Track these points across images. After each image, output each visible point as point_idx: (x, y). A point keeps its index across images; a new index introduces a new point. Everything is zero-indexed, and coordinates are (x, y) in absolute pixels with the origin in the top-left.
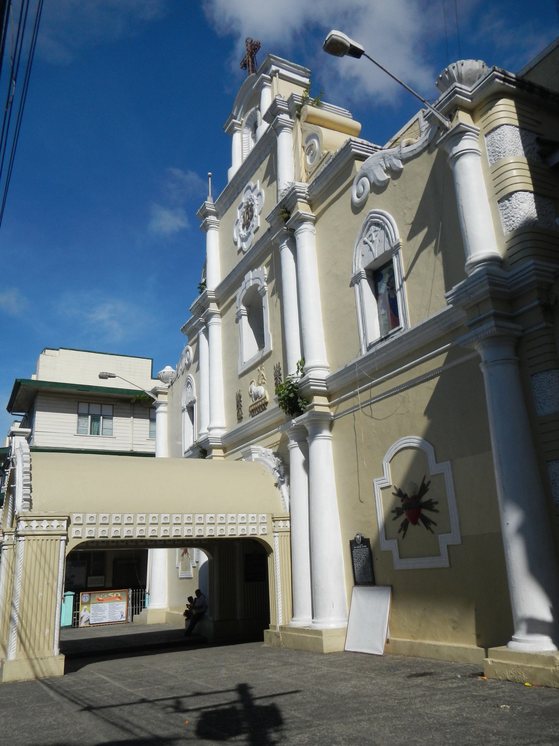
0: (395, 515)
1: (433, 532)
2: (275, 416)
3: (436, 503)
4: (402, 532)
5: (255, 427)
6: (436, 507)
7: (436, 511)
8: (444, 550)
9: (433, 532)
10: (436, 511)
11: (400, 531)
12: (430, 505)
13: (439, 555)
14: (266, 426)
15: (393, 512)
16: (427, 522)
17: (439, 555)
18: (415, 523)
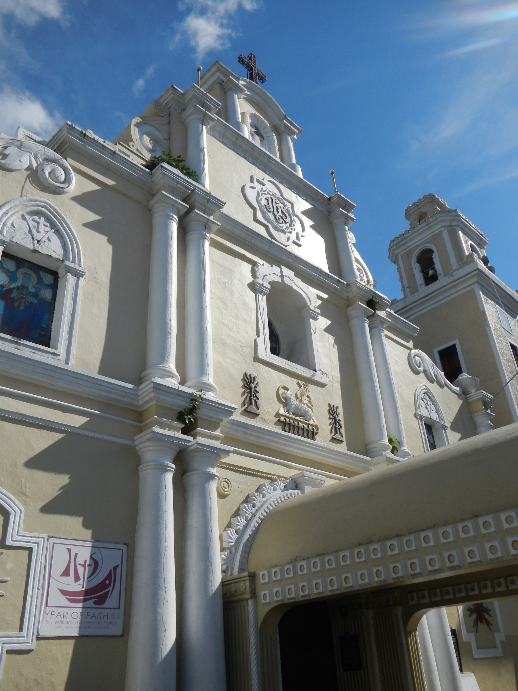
0: (469, 613)
1: (491, 630)
2: (343, 461)
3: (490, 610)
4: (475, 628)
5: (282, 444)
6: (491, 613)
7: (491, 616)
8: (499, 644)
9: (491, 630)
10: (491, 616)
11: (474, 627)
12: (487, 611)
13: (495, 647)
14: (320, 461)
15: (468, 610)
16: (488, 623)
17: (495, 647)
18: (482, 622)
